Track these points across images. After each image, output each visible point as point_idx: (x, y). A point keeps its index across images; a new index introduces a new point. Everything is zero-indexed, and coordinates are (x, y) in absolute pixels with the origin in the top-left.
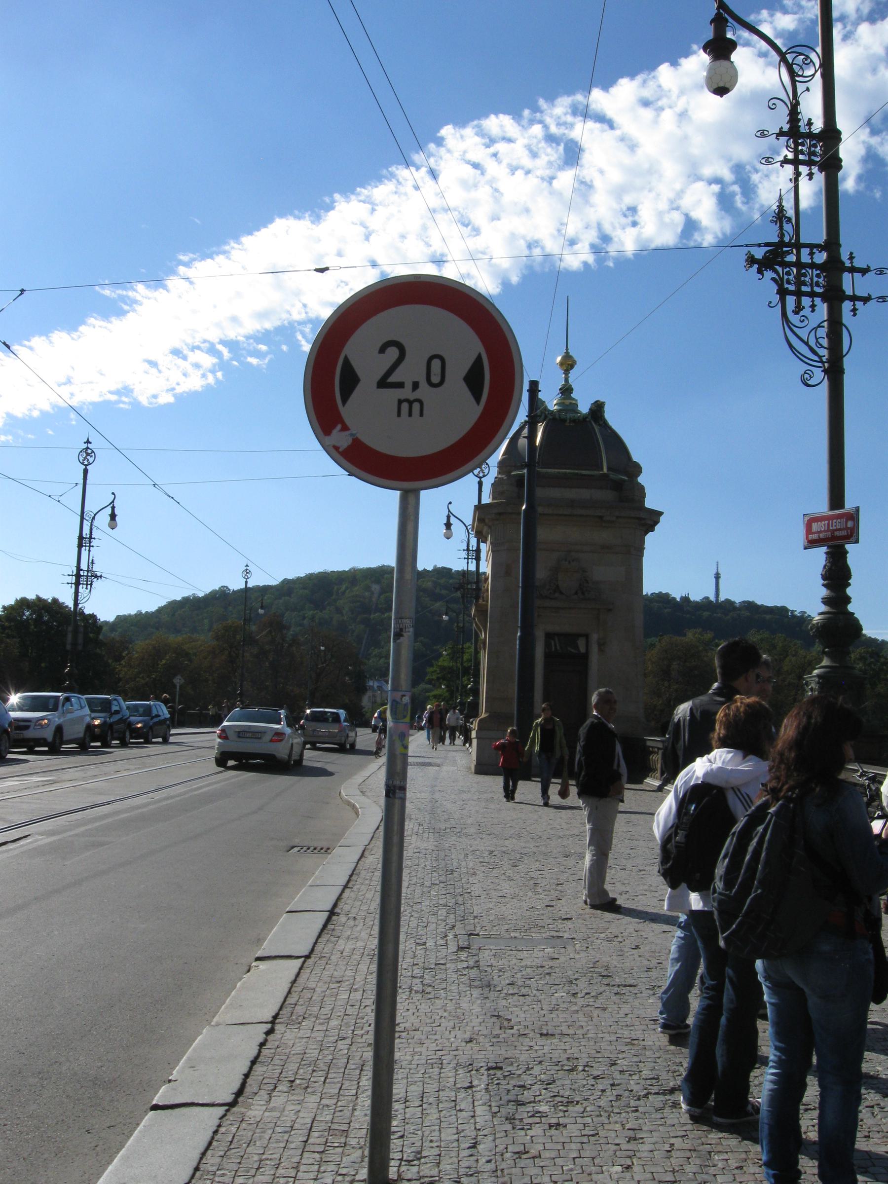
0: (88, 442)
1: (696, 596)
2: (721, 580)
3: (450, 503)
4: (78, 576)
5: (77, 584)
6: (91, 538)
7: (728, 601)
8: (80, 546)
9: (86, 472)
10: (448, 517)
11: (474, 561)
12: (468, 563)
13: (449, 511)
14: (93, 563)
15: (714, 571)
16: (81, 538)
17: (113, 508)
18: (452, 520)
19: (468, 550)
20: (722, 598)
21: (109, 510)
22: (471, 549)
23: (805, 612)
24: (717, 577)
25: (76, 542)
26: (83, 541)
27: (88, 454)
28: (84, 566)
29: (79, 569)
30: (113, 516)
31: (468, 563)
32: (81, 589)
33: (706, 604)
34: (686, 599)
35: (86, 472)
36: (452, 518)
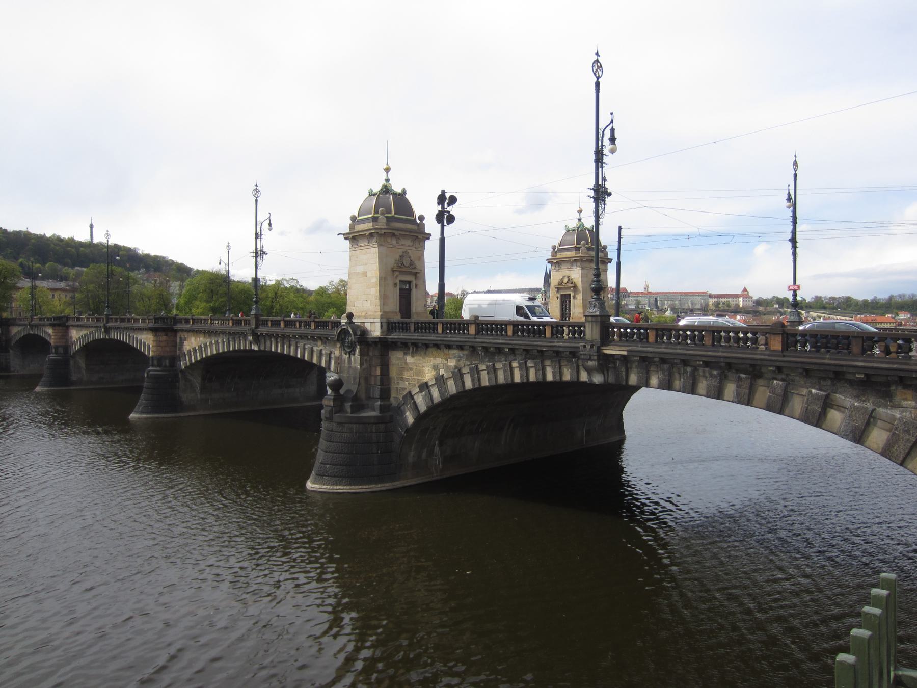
0: (256, 185)
2: (94, 229)
4: (256, 253)
5: (256, 257)
6: (261, 234)
8: (256, 238)
9: (256, 201)
14: (263, 247)
16: (256, 234)
17: (270, 220)
21: (268, 222)
25: (254, 236)
26: (258, 236)
27: (257, 192)
28: (259, 247)
29: (256, 249)
30: (270, 224)
32: (259, 259)
35: (256, 201)
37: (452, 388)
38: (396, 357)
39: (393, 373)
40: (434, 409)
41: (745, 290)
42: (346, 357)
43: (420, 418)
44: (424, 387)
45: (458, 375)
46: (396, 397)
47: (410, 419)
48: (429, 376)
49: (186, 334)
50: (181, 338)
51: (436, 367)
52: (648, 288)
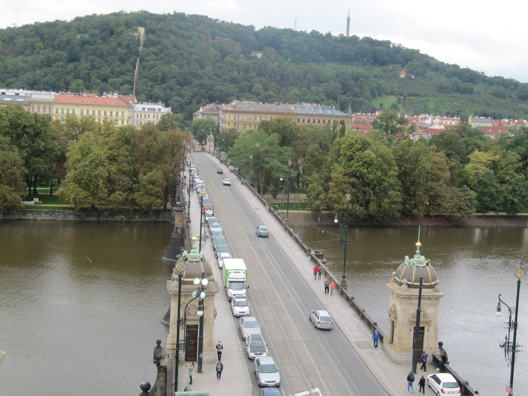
1: (335, 34)
3: (500, 295)
7: (355, 38)
10: (499, 304)
11: (513, 329)
12: (509, 331)
13: (500, 299)
15: (347, 16)
18: (502, 306)
19: (510, 323)
20: (351, 35)
22: (511, 322)
23: (401, 45)
24: (348, 21)
31: (509, 331)
33: (343, 40)
34: (329, 35)
36: (502, 304)
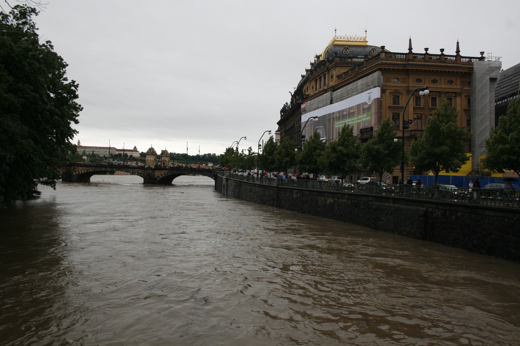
37: (167, 175)
38: (156, 171)
39: (156, 173)
40: (163, 178)
41: (135, 147)
42: (148, 171)
43: (160, 179)
44: (161, 175)
45: (168, 173)
46: (156, 176)
47: (159, 179)
48: (162, 173)
49: (76, 167)
50: (73, 168)
51: (164, 172)
52: (80, 143)
